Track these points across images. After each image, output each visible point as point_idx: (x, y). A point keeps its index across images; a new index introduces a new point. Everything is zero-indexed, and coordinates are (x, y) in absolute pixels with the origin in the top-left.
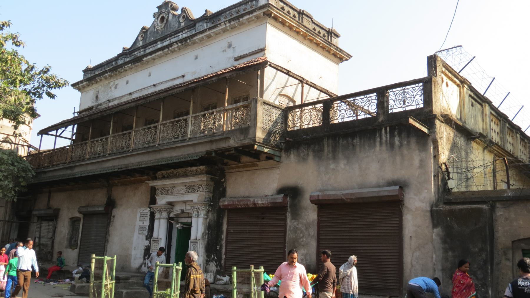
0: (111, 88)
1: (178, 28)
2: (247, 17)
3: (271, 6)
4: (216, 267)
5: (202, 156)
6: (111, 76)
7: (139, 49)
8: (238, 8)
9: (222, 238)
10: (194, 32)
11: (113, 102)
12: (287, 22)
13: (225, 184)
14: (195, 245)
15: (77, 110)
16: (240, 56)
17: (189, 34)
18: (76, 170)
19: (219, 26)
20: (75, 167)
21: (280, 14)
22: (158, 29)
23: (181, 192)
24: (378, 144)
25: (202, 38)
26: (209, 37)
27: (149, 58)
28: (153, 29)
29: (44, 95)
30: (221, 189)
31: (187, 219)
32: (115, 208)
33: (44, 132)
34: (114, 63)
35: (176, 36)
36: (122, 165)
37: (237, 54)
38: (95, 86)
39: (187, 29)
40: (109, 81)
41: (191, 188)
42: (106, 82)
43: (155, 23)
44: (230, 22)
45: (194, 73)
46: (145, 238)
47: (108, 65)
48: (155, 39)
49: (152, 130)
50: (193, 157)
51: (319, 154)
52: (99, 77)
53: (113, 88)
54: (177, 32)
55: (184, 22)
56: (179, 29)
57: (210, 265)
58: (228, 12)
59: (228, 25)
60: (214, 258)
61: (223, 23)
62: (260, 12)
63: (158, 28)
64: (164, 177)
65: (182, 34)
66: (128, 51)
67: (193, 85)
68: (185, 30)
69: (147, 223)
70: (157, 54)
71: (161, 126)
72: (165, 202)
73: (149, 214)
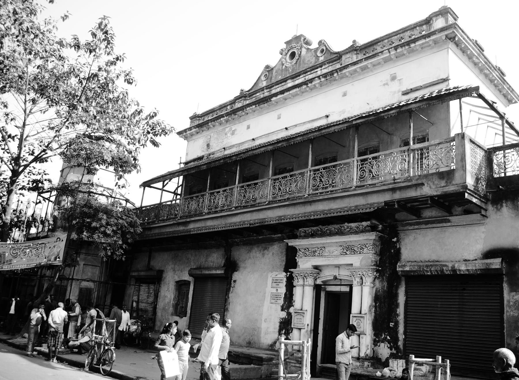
0: (226, 134)
1: (315, 63)
2: (423, 41)
3: (457, 27)
4: (389, 349)
5: (378, 208)
6: (227, 121)
7: (262, 89)
8: (402, 35)
9: (398, 312)
10: (338, 66)
11: (230, 150)
12: (469, 49)
13: (398, 244)
14: (359, 321)
15: (184, 161)
16: (411, 89)
17: (330, 69)
18: (191, 226)
19: (380, 54)
21: (464, 39)
22: (287, 66)
23: (334, 254)
25: (355, 71)
27: (279, 98)
28: (281, 67)
29: (148, 143)
30: (392, 251)
31: (340, 287)
32: (236, 271)
33: (147, 184)
34: (229, 107)
35: (312, 72)
36: (255, 220)
37: (404, 89)
38: (205, 133)
40: (225, 127)
41: (349, 249)
42: (221, 128)
43: (283, 60)
44: (396, 50)
45: (343, 112)
46: (279, 308)
47: (222, 110)
48: (283, 78)
49: (297, 178)
50: (322, 215)
52: (213, 123)
53: (229, 135)
54: (314, 68)
55: (323, 56)
56: (316, 64)
57: (379, 346)
58: (386, 41)
59: (393, 52)
61: (387, 51)
62: (441, 35)
63: (288, 65)
64: (307, 236)
65: (321, 70)
66: (248, 93)
67: (358, 121)
68: (325, 64)
69: (283, 290)
70: (291, 92)
71: (310, 172)
72: (311, 267)
73: (285, 279)
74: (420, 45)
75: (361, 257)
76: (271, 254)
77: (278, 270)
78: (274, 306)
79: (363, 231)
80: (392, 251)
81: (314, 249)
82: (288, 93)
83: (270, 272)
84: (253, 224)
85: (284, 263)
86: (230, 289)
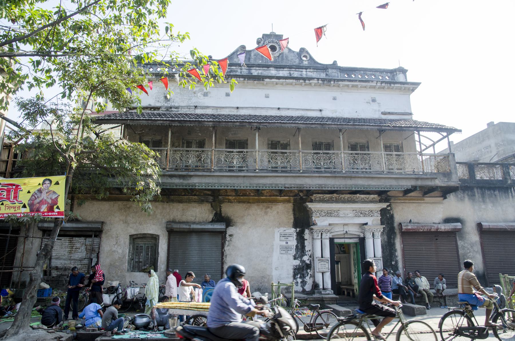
2: (399, 85)
11: (205, 110)
16: (389, 113)
20: (191, 176)
23: (348, 216)
24: (511, 197)
25: (348, 86)
26: (356, 86)
30: (388, 215)
31: (344, 239)
32: (232, 226)
36: (291, 184)
39: (313, 69)
44: (381, 83)
47: (181, 66)
51: (472, 197)
59: (379, 84)
60: (390, 272)
68: (311, 69)
70: (287, 81)
73: (295, 234)
74: (396, 87)
75: (372, 218)
76: (275, 212)
77: (287, 226)
78: (285, 256)
79: (372, 202)
80: (388, 215)
81: (331, 211)
82: (284, 80)
83: (277, 228)
84: (288, 188)
85: (292, 221)
86: (225, 242)
